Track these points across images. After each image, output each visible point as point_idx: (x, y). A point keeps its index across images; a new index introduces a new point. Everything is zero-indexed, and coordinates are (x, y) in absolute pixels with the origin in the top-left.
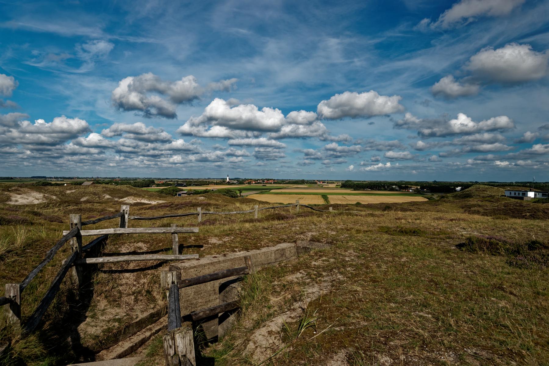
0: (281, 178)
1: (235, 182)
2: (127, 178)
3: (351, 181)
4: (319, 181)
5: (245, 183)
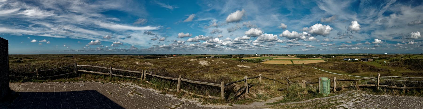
0: (274, 54)
1: (259, 56)
3: (300, 55)
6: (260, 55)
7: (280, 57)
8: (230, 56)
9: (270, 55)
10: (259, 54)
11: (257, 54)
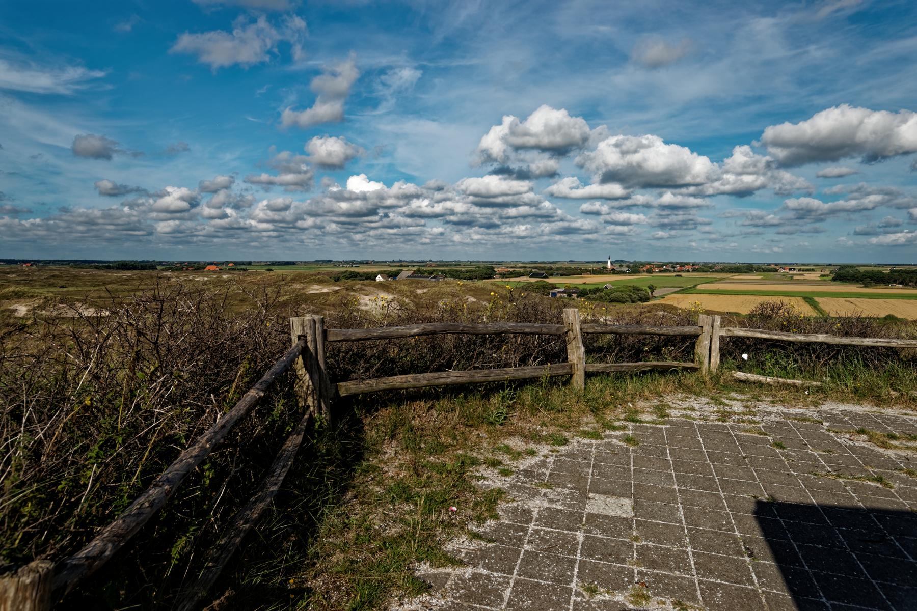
1: (625, 269)
2: (442, 261)
4: (783, 265)
5: (642, 270)
6: (628, 267)
7: (737, 277)
8: (488, 272)
9: (679, 267)
10: (620, 263)
11: (611, 263)
